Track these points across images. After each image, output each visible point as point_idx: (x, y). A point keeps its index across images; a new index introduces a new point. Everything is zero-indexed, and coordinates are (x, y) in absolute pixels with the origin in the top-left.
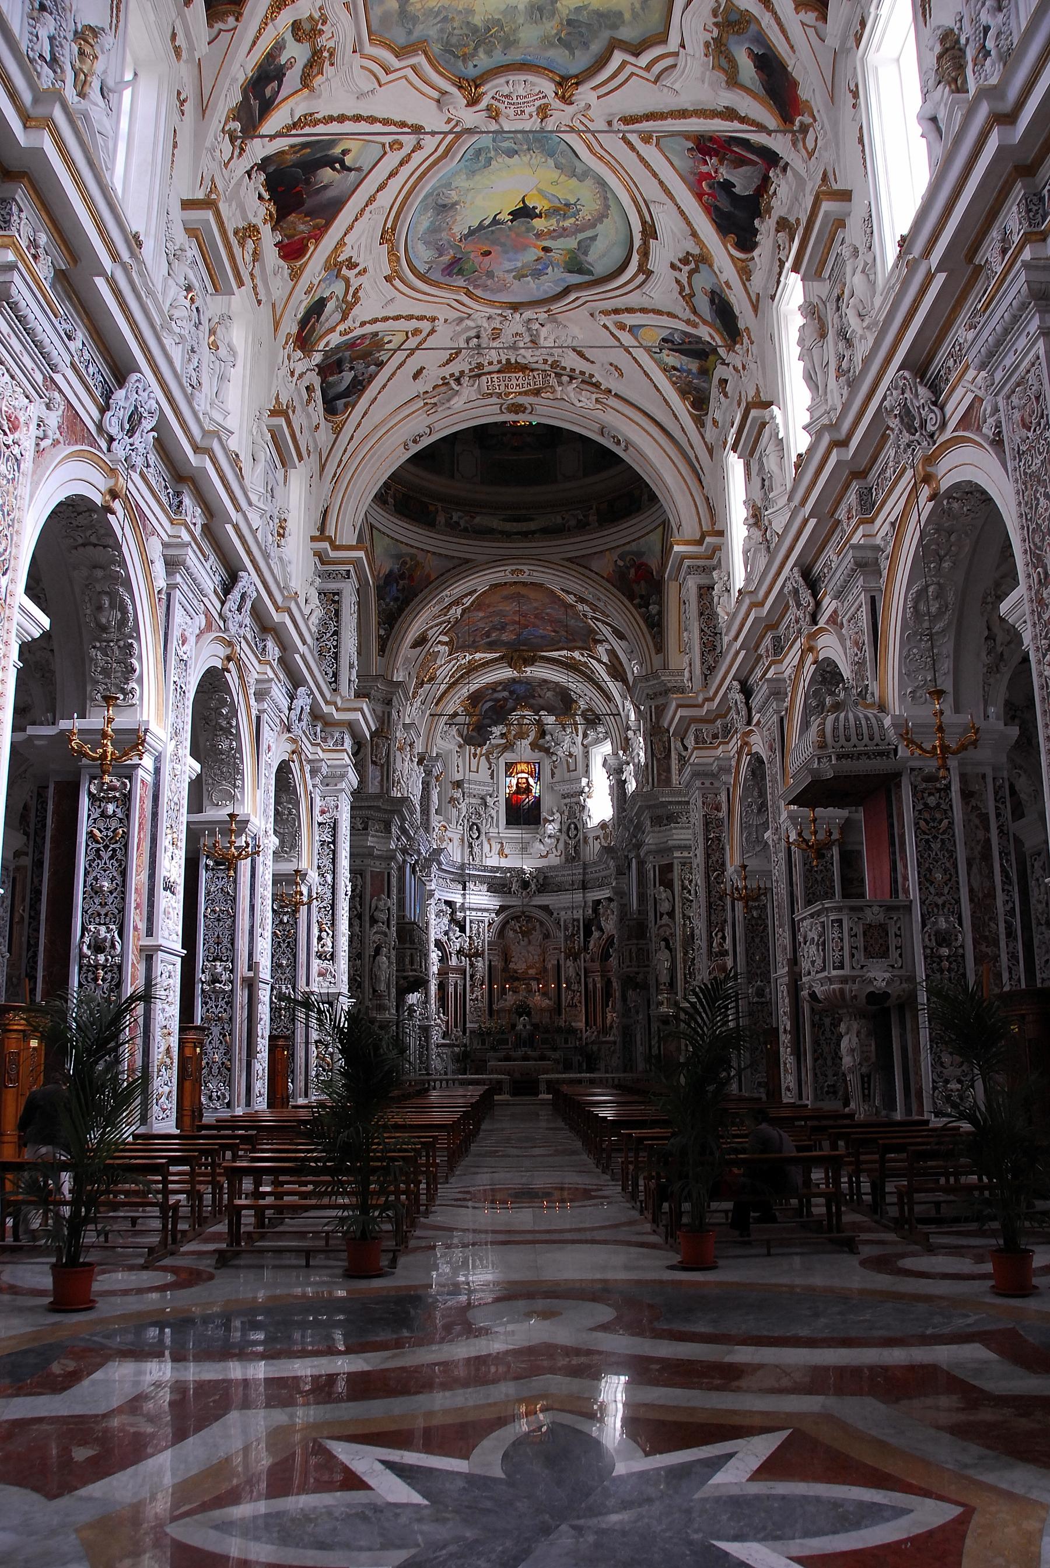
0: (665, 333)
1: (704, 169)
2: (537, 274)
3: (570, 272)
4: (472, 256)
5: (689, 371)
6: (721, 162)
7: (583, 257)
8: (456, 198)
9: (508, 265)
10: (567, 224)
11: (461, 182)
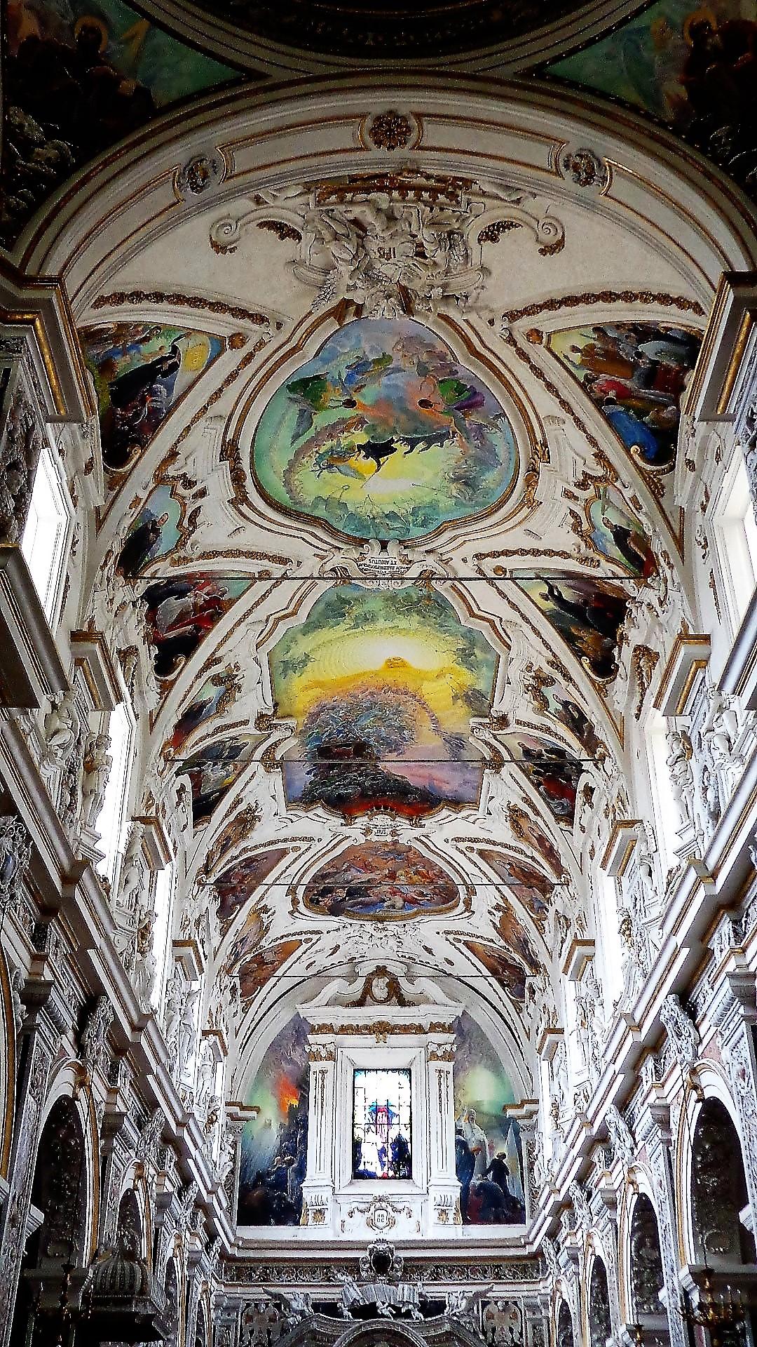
0: (181, 379)
1: (207, 589)
2: (360, 367)
3: (317, 377)
4: (441, 408)
5: (124, 352)
6: (195, 604)
7: (304, 406)
8: (453, 486)
9: (398, 379)
10: (329, 444)
11: (445, 502)
